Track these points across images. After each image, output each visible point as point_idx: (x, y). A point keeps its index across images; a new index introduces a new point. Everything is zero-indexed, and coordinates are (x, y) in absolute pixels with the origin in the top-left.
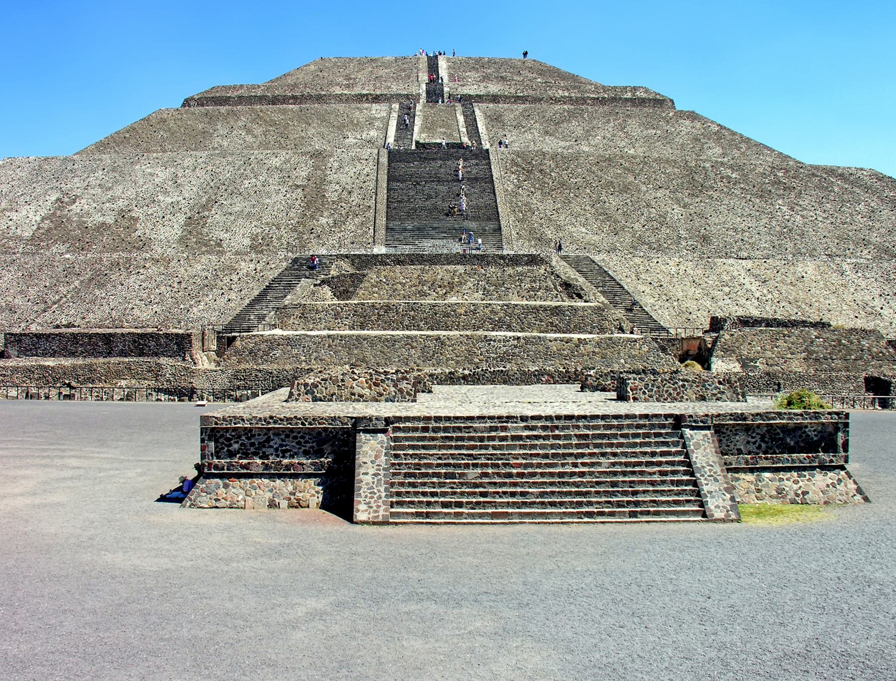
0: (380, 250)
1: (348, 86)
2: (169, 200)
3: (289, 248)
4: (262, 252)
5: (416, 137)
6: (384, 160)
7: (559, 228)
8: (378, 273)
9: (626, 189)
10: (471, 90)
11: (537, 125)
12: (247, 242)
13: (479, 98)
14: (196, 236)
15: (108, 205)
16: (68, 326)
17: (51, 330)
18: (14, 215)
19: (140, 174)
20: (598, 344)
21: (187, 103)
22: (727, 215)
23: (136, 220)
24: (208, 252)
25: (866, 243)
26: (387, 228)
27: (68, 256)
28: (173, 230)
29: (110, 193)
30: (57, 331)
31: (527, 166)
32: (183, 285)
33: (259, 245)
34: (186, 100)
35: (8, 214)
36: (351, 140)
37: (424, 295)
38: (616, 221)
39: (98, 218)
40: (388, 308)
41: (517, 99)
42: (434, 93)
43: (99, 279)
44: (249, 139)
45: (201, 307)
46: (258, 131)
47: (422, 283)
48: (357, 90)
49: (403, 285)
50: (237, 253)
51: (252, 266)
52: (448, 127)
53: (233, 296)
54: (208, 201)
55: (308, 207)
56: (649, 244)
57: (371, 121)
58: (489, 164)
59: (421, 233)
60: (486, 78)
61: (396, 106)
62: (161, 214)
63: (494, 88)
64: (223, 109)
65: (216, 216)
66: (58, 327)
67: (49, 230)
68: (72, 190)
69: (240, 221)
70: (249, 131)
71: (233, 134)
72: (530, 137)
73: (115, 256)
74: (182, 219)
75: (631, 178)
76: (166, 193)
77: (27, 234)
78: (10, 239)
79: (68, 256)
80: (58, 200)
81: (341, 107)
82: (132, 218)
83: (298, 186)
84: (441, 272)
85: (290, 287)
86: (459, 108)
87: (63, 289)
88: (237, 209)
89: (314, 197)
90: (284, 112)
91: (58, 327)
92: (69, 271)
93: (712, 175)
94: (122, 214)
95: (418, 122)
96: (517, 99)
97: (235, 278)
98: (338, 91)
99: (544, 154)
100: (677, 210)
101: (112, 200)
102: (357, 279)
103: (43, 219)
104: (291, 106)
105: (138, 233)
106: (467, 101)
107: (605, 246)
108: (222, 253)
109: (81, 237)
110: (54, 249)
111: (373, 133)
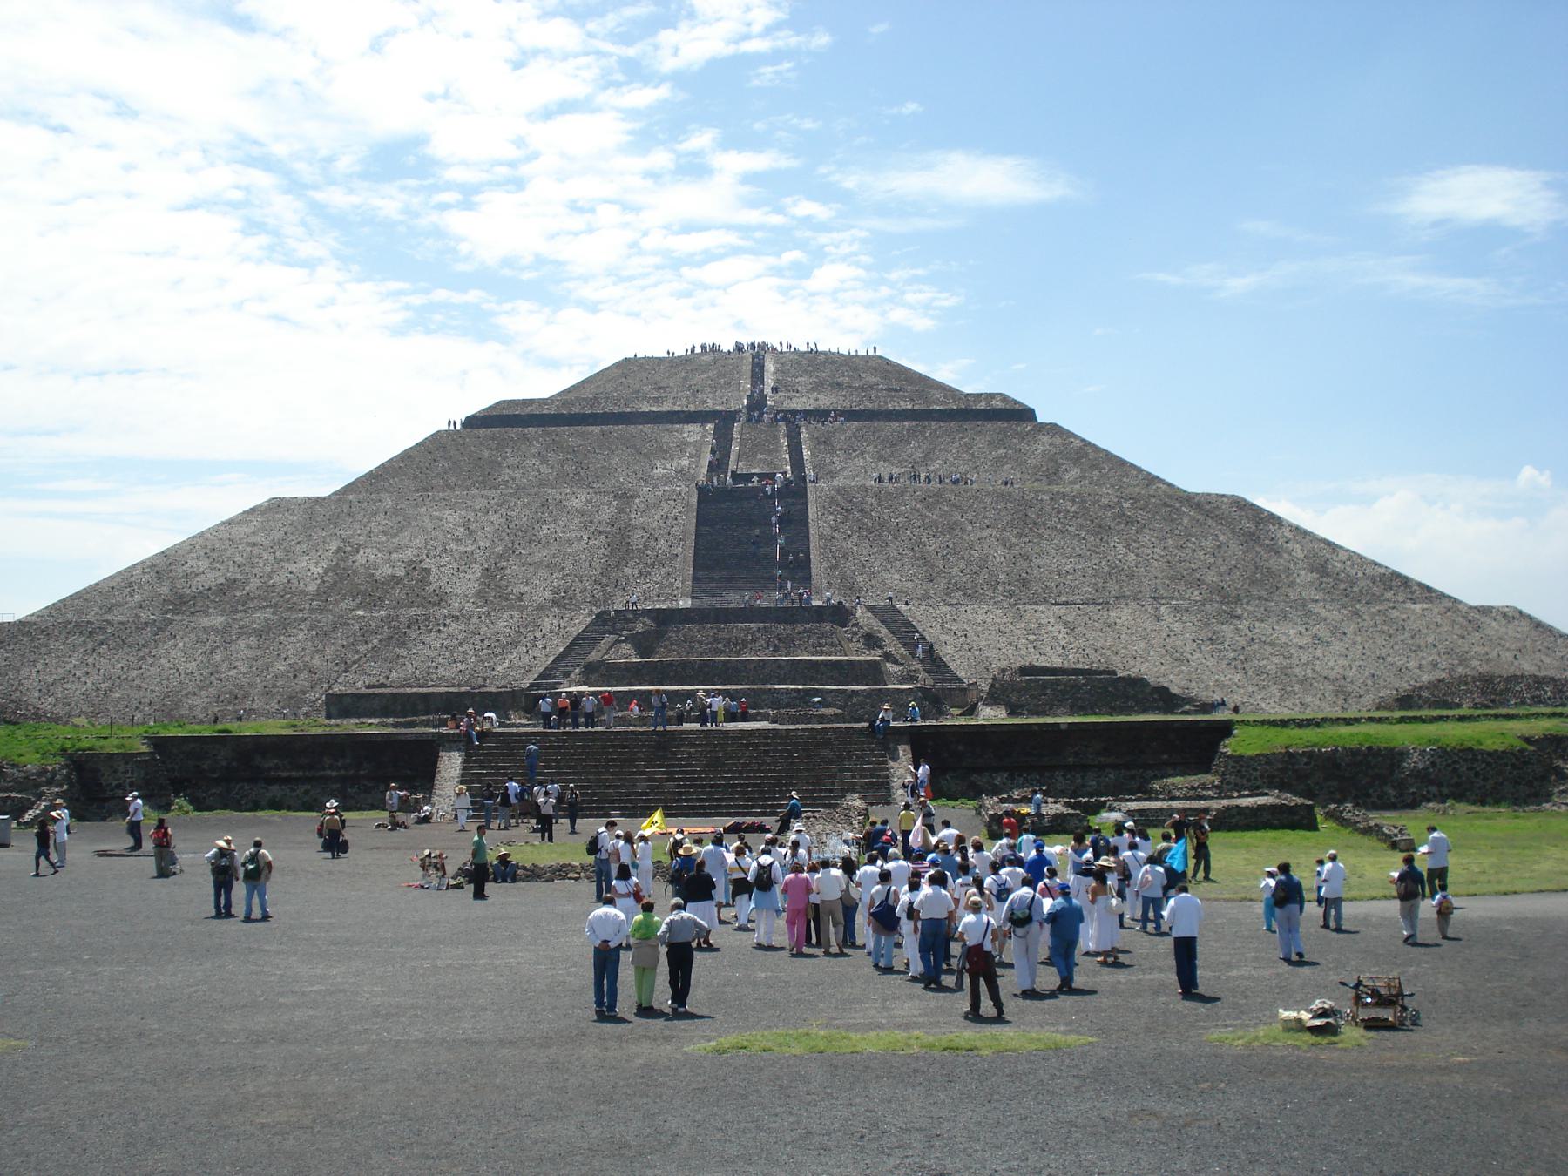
0: (685, 603)
1: (656, 401)
2: (463, 549)
3: (594, 603)
5: (732, 466)
6: (694, 500)
7: (873, 575)
8: (678, 631)
9: (951, 528)
10: (802, 403)
11: (871, 448)
12: (548, 595)
13: (807, 414)
14: (494, 591)
15: (395, 555)
16: (383, 685)
17: (364, 691)
18: (293, 567)
19: (426, 519)
20: (869, 694)
21: (472, 422)
22: (1057, 557)
23: (428, 571)
24: (511, 608)
25: (1199, 583)
26: (695, 579)
27: (360, 613)
29: (396, 540)
30: (370, 691)
31: (846, 504)
32: (487, 643)
33: (563, 601)
34: (468, 418)
35: (286, 565)
36: (659, 471)
37: (719, 652)
38: (934, 566)
39: (386, 570)
40: (684, 664)
41: (851, 415)
42: (757, 404)
43: (398, 638)
44: (544, 469)
45: (506, 664)
46: (553, 458)
47: (717, 641)
48: (666, 407)
49: (700, 643)
50: (540, 608)
51: (556, 622)
52: (769, 452)
53: (537, 652)
54: (506, 549)
55: (611, 556)
56: (964, 590)
57: (682, 446)
58: (806, 504)
59: (729, 583)
60: (818, 387)
61: (710, 427)
62: (455, 565)
63: (825, 401)
64: (513, 432)
65: (514, 568)
66: (374, 686)
67: (334, 584)
68: (352, 536)
69: (540, 572)
70: (544, 460)
71: (527, 462)
72: (860, 462)
73: (412, 611)
74: (478, 570)
75: (957, 516)
76: (458, 540)
77: (312, 587)
78: (294, 594)
79: (360, 613)
80: (339, 549)
81: (648, 428)
82: (424, 570)
83: (600, 533)
84: (740, 629)
85: (595, 643)
86: (783, 427)
87: (363, 649)
88: (536, 559)
89: (620, 545)
90: (582, 435)
91: (374, 686)
92: (366, 633)
93: (1048, 509)
94: (412, 565)
95: (735, 448)
96: (851, 415)
97: (539, 634)
98: (645, 408)
99: (866, 489)
100: (1001, 551)
101: (399, 548)
102: (659, 635)
103: (326, 571)
104: (591, 428)
105: (433, 586)
106: (791, 419)
107: (920, 593)
108: (524, 608)
109: (373, 593)
110: (344, 605)
111: (685, 462)
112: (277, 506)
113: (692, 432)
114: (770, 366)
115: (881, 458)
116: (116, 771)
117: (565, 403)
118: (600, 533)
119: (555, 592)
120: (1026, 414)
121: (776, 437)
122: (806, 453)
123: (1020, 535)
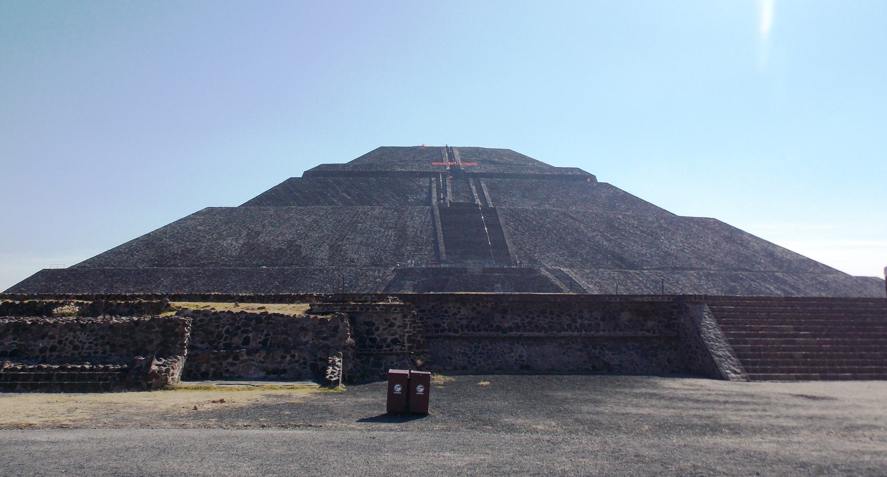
1: (403, 166)
4: (378, 265)
13: (482, 175)
28: (323, 253)
48: (408, 169)
60: (483, 161)
70: (349, 194)
80: (248, 234)
86: (471, 181)
99: (527, 210)
106: (475, 176)
112: (210, 212)
113: (424, 182)
114: (456, 153)
115: (524, 197)
116: (392, 325)
117: (355, 166)
118: (391, 228)
119: (372, 258)
120: (593, 178)
121: (468, 183)
122: (486, 194)
123: (612, 235)
